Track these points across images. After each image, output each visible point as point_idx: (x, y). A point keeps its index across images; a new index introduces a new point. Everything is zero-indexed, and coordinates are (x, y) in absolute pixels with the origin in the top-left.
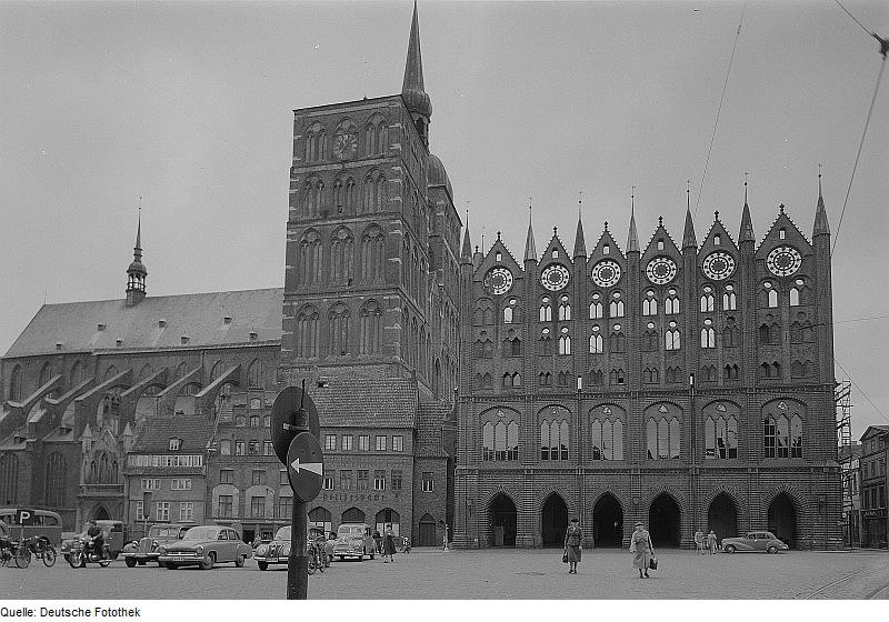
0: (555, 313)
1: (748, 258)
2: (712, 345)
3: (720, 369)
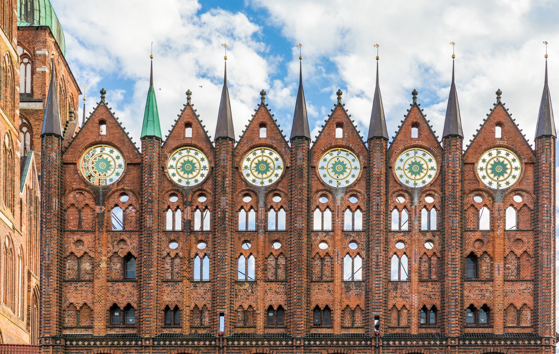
2: (404, 277)
3: (415, 312)
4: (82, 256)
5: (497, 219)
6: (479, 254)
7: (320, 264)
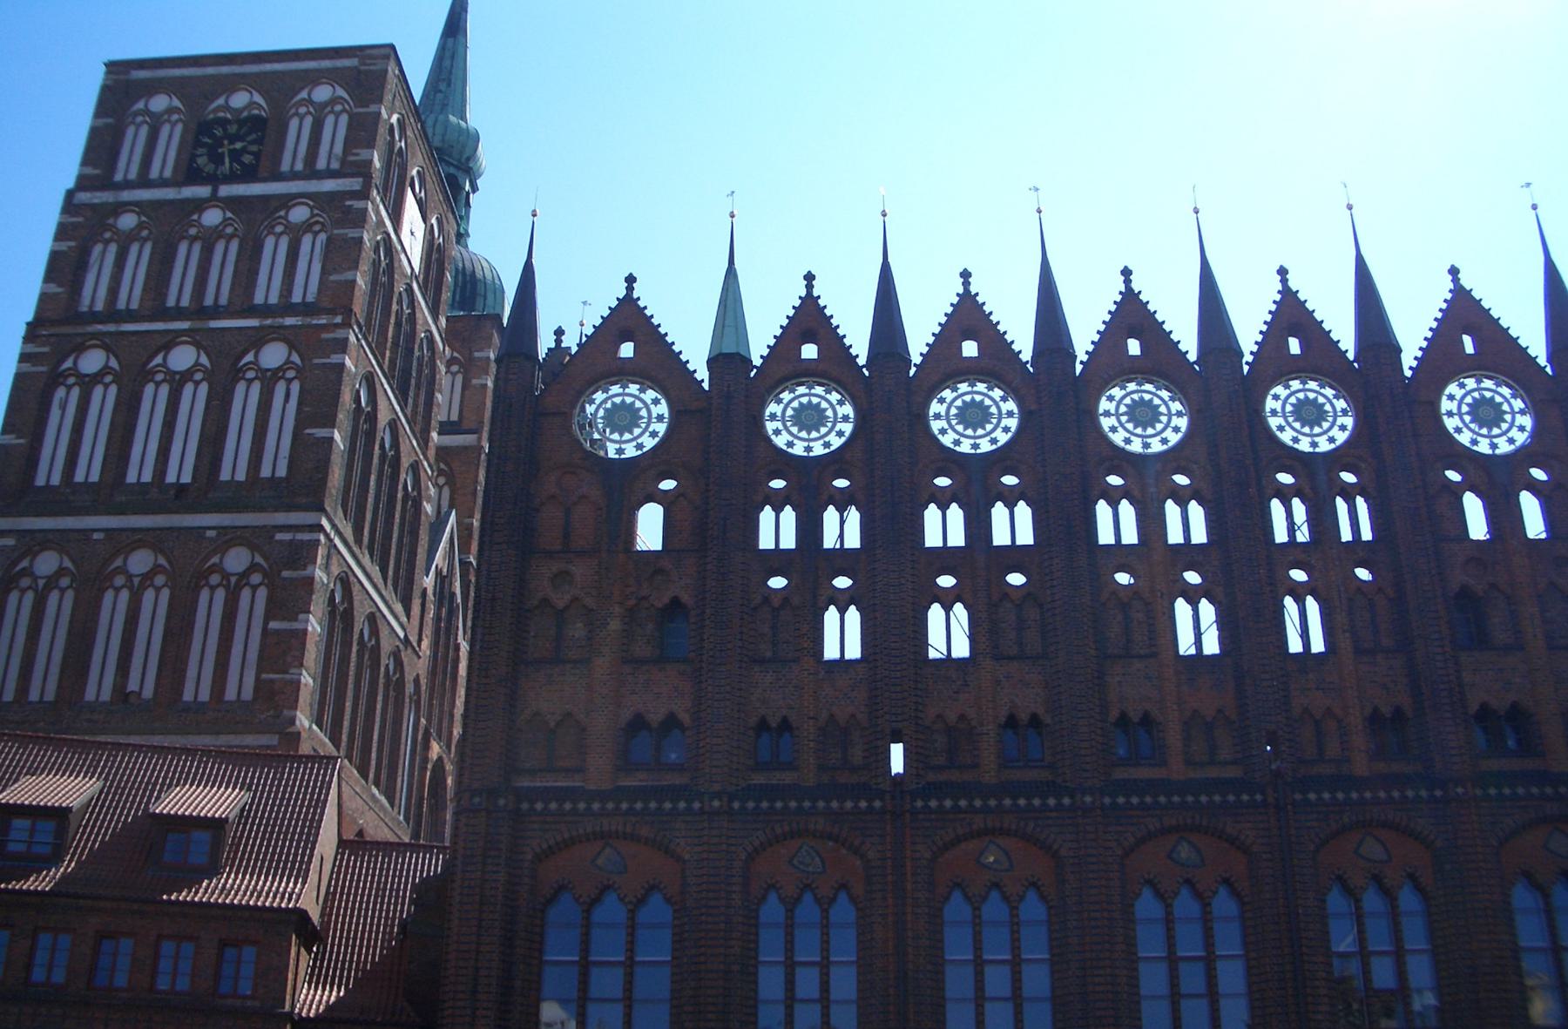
5: (1504, 516)
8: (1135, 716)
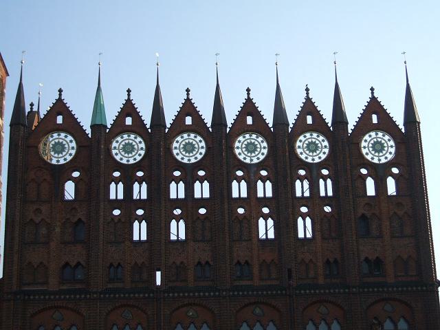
0: (128, 191)
1: (343, 141)
2: (309, 235)
3: (320, 264)
4: (40, 222)
5: (381, 186)
6: (368, 214)
7: (239, 226)
8: (242, 262)
